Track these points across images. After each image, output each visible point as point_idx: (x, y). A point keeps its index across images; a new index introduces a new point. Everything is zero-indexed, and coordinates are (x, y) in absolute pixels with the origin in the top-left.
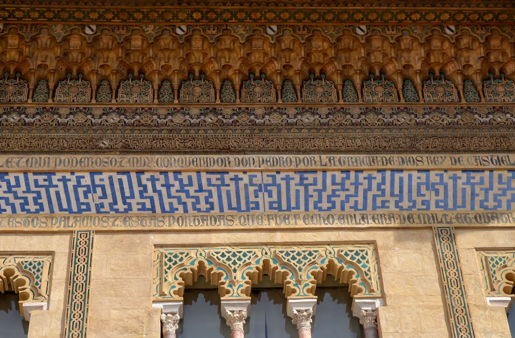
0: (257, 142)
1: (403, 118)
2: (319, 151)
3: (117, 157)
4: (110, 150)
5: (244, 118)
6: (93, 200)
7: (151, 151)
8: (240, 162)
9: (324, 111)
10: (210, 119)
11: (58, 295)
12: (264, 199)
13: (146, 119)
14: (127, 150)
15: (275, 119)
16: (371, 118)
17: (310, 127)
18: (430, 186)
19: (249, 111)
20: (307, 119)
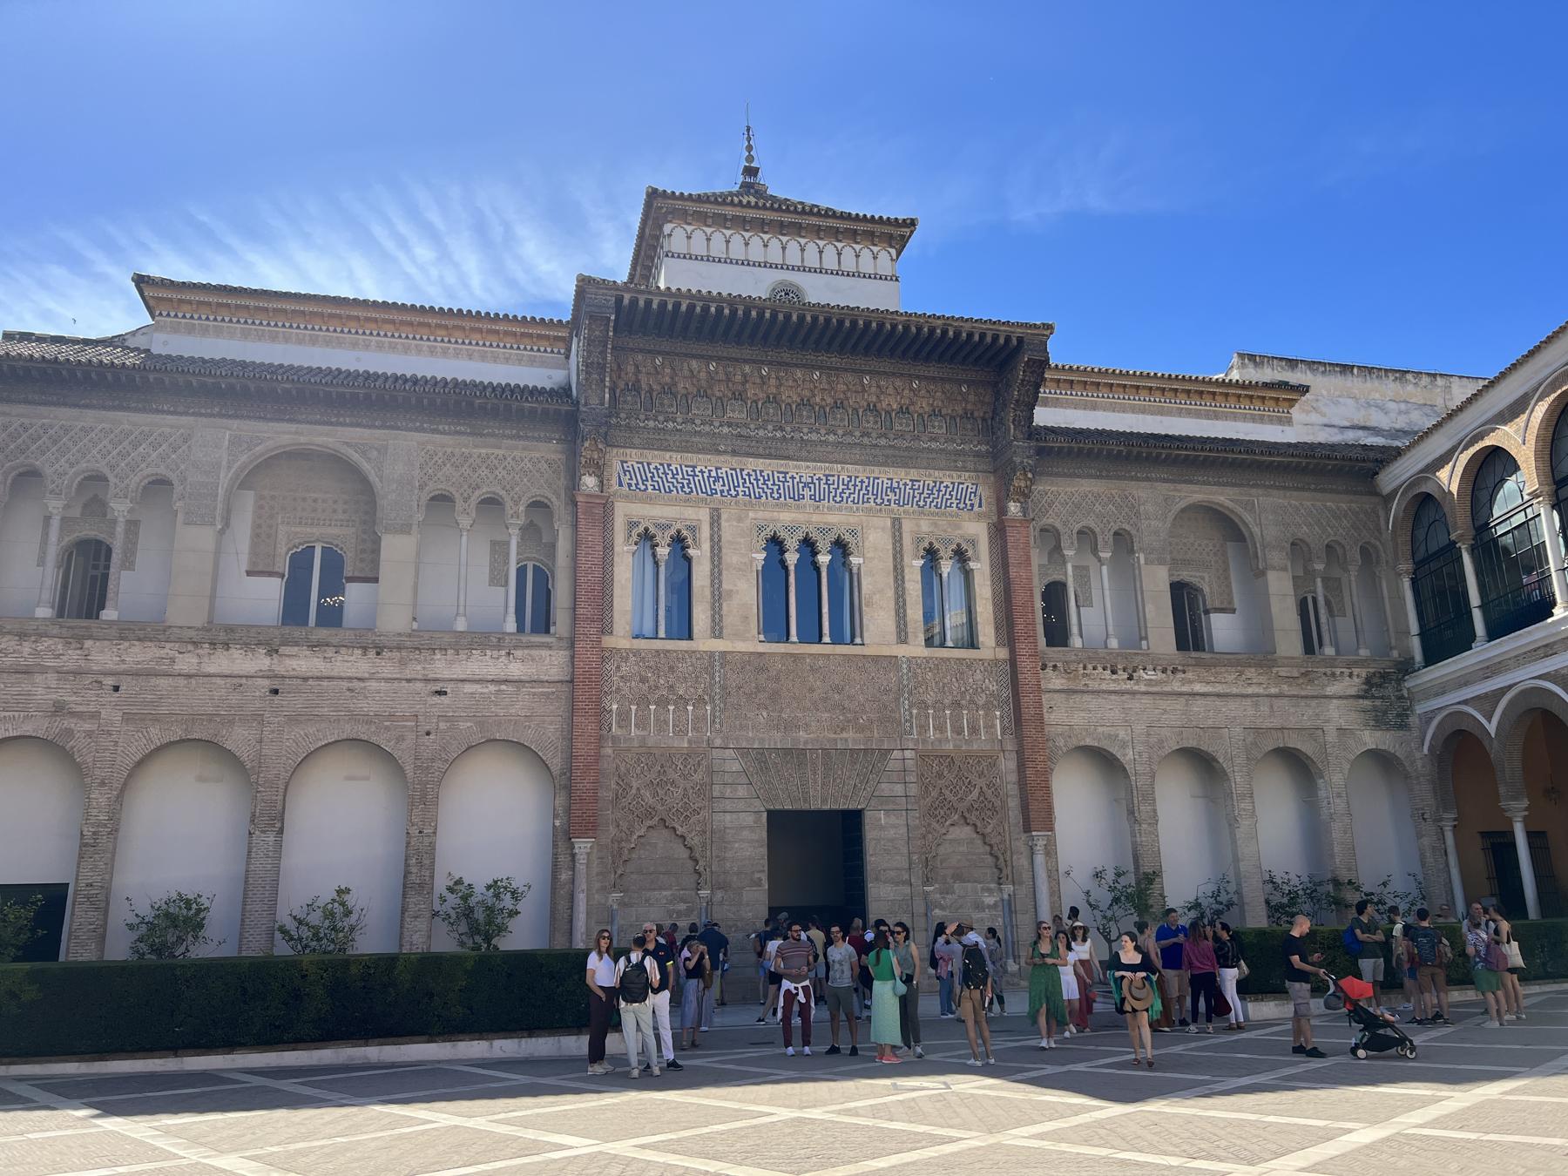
0: (804, 454)
1: (883, 442)
2: (837, 462)
3: (728, 458)
4: (725, 452)
5: (797, 435)
6: (718, 486)
9: (840, 432)
11: (706, 546)
12: (807, 492)
13: (744, 432)
14: (734, 453)
15: (814, 437)
16: (866, 440)
17: (833, 444)
18: (893, 490)
20: (831, 438)
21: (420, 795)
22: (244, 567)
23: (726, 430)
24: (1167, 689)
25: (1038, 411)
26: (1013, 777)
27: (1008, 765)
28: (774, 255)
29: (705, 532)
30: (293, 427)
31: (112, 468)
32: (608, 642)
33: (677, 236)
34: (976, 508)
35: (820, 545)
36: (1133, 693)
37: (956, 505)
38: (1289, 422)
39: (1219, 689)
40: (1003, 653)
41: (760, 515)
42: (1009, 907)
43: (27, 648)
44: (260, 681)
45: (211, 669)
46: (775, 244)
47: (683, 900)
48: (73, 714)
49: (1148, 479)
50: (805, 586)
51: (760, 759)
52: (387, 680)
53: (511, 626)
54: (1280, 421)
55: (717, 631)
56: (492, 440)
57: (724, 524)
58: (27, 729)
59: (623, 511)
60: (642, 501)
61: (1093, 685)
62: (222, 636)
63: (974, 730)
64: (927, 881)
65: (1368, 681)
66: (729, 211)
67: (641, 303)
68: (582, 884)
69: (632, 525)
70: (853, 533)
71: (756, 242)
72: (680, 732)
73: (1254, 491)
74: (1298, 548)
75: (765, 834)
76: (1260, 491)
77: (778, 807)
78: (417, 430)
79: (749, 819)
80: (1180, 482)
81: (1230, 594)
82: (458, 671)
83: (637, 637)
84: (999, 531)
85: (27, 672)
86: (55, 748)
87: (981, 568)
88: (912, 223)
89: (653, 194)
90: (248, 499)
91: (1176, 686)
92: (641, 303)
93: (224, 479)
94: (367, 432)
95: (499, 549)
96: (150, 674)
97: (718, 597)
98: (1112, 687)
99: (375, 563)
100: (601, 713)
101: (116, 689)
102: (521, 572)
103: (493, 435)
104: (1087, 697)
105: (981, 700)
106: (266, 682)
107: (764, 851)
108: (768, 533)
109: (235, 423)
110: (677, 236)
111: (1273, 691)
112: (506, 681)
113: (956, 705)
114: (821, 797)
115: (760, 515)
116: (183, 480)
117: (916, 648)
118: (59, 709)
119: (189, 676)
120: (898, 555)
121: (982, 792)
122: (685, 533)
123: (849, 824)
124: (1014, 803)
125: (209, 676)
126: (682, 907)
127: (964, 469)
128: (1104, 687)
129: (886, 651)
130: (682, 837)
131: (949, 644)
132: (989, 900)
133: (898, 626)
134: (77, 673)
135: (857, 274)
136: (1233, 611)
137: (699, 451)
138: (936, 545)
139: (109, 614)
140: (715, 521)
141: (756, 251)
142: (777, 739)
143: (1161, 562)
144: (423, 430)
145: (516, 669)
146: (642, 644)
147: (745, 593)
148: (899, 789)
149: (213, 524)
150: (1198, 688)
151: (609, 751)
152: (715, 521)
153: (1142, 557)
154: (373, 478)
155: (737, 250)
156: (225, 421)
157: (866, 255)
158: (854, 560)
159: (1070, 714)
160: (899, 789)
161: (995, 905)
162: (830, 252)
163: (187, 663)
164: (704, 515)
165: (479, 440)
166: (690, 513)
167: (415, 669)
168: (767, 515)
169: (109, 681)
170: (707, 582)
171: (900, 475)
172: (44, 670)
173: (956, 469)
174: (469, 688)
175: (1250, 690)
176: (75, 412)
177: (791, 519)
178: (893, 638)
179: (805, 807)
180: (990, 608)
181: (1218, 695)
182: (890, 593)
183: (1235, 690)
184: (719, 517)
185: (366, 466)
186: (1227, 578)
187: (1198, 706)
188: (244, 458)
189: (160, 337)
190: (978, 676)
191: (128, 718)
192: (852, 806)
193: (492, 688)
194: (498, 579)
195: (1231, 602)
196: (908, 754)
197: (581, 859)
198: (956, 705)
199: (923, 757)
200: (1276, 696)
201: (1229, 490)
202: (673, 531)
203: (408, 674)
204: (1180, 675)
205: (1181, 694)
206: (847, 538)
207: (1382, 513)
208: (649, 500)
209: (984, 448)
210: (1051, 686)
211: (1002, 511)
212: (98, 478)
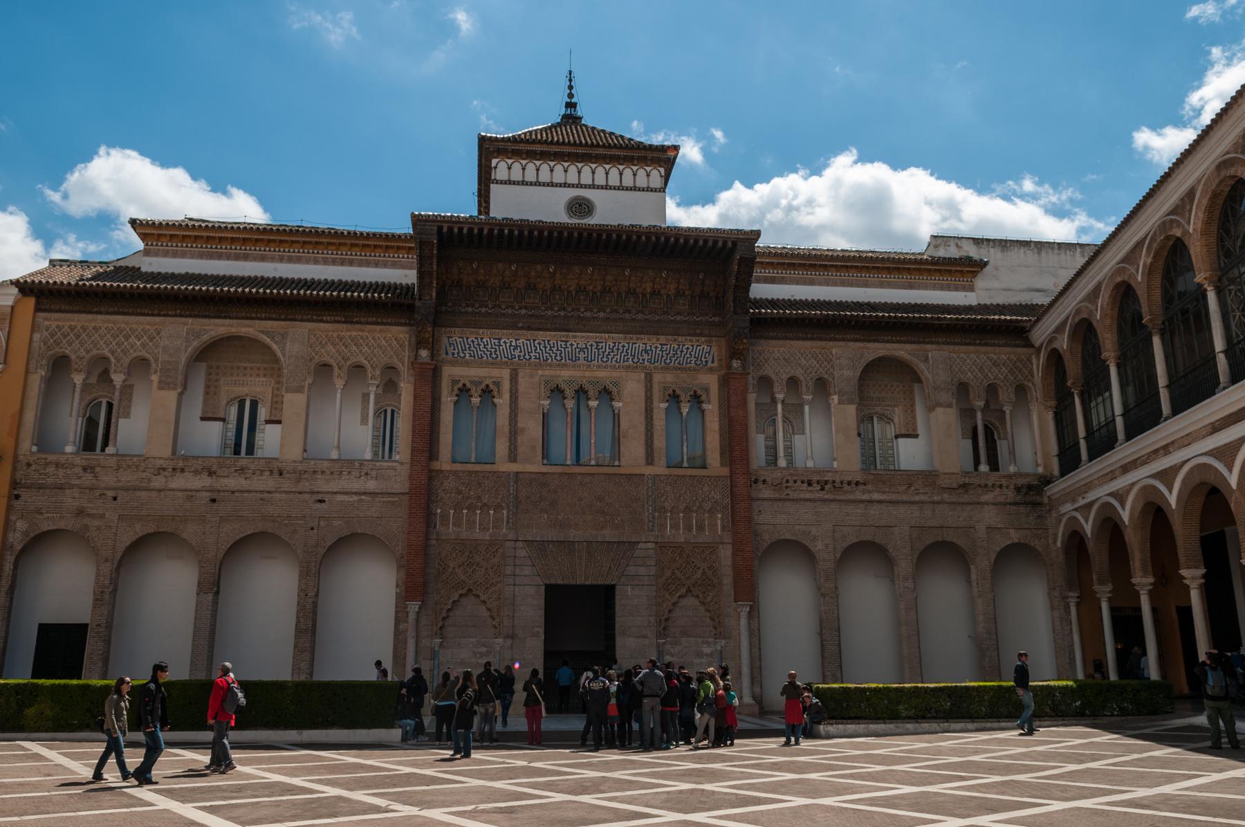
1: (640, 316)
5: (575, 314)
6: (517, 353)
7: (539, 329)
8: (574, 337)
10: (562, 313)
11: (507, 396)
12: (582, 356)
14: (529, 328)
15: (588, 314)
16: (627, 316)
18: (646, 351)
19: (578, 310)
20: (601, 315)
22: (199, 414)
23: (523, 312)
24: (852, 497)
26: (729, 562)
27: (726, 554)
28: (572, 177)
29: (506, 386)
30: (227, 321)
31: (113, 353)
32: (436, 465)
33: (501, 168)
34: (710, 364)
35: (591, 393)
36: (824, 501)
38: (972, 289)
39: (893, 497)
40: (725, 471)
41: (547, 373)
43: (61, 472)
44: (205, 494)
45: (173, 485)
47: (484, 645)
48: (89, 515)
49: (843, 340)
51: (539, 547)
52: (286, 492)
54: (964, 289)
55: (513, 458)
56: (359, 326)
57: (520, 380)
59: (449, 372)
60: (462, 365)
61: (793, 495)
62: (181, 464)
63: (701, 528)
65: (1018, 489)
66: (538, 148)
67: (456, 230)
69: (454, 382)
70: (616, 384)
71: (559, 169)
73: (929, 347)
74: (963, 389)
75: (543, 601)
76: (934, 347)
77: (553, 582)
78: (308, 321)
80: (869, 341)
81: (915, 424)
82: (334, 486)
83: (454, 462)
84: (725, 382)
85: (61, 488)
87: (712, 408)
89: (482, 140)
90: (202, 368)
91: (859, 496)
92: (456, 230)
93: (183, 359)
94: (275, 323)
96: (136, 489)
97: (514, 432)
98: (808, 496)
101: (115, 499)
103: (360, 323)
104: (787, 504)
105: (707, 506)
106: (208, 494)
107: (542, 612)
109: (190, 320)
110: (501, 168)
111: (936, 498)
112: (364, 493)
113: (688, 510)
114: (583, 575)
115: (547, 373)
116: (156, 360)
118: (80, 512)
119: (159, 491)
120: (649, 399)
121: (704, 573)
122: (491, 386)
123: (608, 593)
124: (728, 581)
125: (172, 490)
126: (484, 649)
127: (701, 335)
128: (802, 496)
130: (484, 602)
131: (685, 464)
132: (707, 650)
133: (647, 452)
134: (92, 489)
135: (635, 188)
136: (916, 436)
137: (503, 328)
138: (678, 392)
139: (110, 450)
140: (514, 378)
141: (559, 176)
142: (552, 535)
143: (850, 402)
144: (313, 321)
145: (371, 485)
146: (458, 467)
149: (175, 389)
150: (876, 496)
151: (434, 542)
152: (514, 378)
153: (836, 398)
154: (279, 354)
155: (545, 176)
156: (183, 319)
157: (641, 173)
160: (642, 571)
161: (711, 654)
163: (158, 482)
164: (505, 374)
165: (349, 326)
166: (496, 372)
167: (304, 485)
168: (552, 373)
169: (111, 494)
170: (507, 422)
172: (72, 487)
173: (695, 335)
174: (340, 498)
175: (917, 498)
176: (90, 316)
178: (643, 461)
179: (573, 582)
180: (717, 437)
181: (891, 502)
182: (642, 428)
183: (904, 498)
184: (517, 375)
185: (274, 347)
186: (913, 411)
187: (874, 510)
188: (195, 343)
189: (148, 259)
190: (706, 489)
191: (121, 518)
192: (608, 582)
193: (355, 498)
195: (915, 429)
196: (650, 545)
198: (688, 510)
199: (662, 546)
200: (938, 503)
201: (908, 347)
202: (483, 386)
203: (300, 487)
204: (861, 487)
205: (861, 501)
207: (1034, 361)
208: (467, 364)
209: (717, 319)
210: (761, 496)
211: (729, 367)
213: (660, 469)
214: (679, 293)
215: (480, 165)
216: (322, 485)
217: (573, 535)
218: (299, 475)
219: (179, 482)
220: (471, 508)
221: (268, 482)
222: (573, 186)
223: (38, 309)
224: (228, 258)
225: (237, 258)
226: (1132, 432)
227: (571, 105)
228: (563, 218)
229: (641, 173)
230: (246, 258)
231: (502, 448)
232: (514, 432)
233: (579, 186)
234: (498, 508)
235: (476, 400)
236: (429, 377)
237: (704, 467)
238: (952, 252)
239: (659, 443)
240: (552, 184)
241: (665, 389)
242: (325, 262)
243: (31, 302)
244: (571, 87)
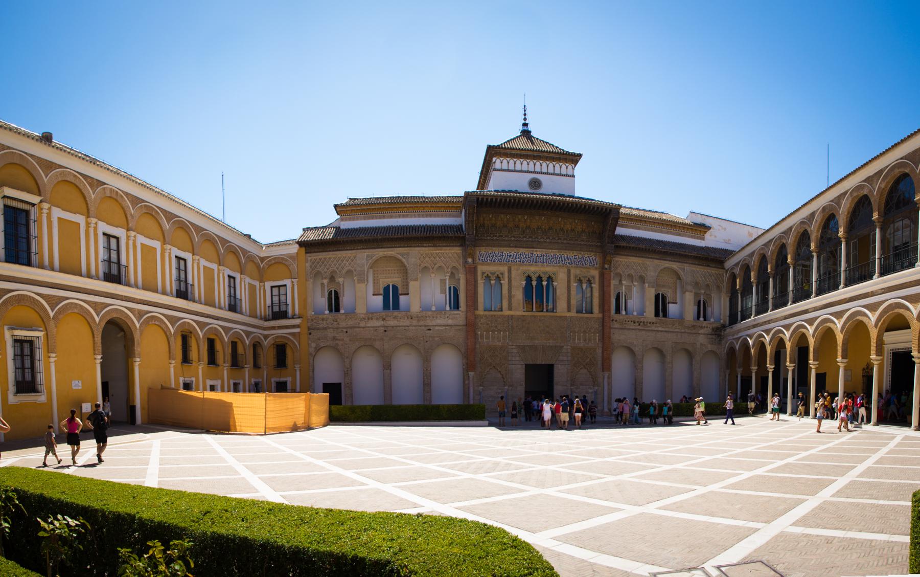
21: (426, 360)
25: (618, 228)
27: (599, 351)
28: (531, 169)
33: (498, 162)
37: (587, 263)
40: (601, 315)
42: (596, 393)
46: (531, 163)
50: (537, 291)
51: (522, 348)
53: (448, 308)
55: (510, 308)
58: (328, 344)
63: (590, 340)
64: (572, 385)
68: (471, 384)
70: (554, 274)
72: (499, 341)
79: (519, 366)
84: (602, 275)
85: (325, 329)
86: (335, 349)
87: (596, 286)
88: (580, 155)
95: (443, 282)
96: (355, 327)
97: (510, 297)
99: (407, 289)
100: (476, 334)
102: (450, 288)
108: (526, 275)
110: (498, 162)
113: (585, 332)
114: (541, 360)
117: (573, 314)
118: (334, 338)
120: (569, 281)
129: (563, 314)
134: (337, 328)
135: (560, 175)
139: (342, 311)
141: (525, 167)
145: (450, 322)
146: (487, 313)
147: (519, 295)
148: (565, 358)
155: (518, 167)
157: (564, 166)
158: (555, 284)
159: (618, 336)
160: (565, 358)
162: (551, 166)
171: (571, 254)
177: (534, 269)
182: (566, 295)
191: (350, 340)
194: (443, 291)
197: (471, 378)
198: (585, 332)
206: (552, 276)
212: (334, 272)
213: (573, 314)
214: (583, 231)
215: (485, 160)
216: (429, 322)
217: (536, 342)
218: (419, 318)
219: (371, 324)
220: (493, 331)
221: (407, 323)
222: (531, 172)
223: (306, 253)
224: (377, 218)
225: (380, 218)
226: (758, 313)
227: (525, 125)
228: (528, 189)
229: (564, 166)
230: (384, 217)
231: (505, 304)
232: (510, 297)
233: (534, 172)
234: (505, 331)
235: (493, 282)
236: (471, 272)
237: (592, 313)
238: (699, 220)
239: (573, 302)
240: (521, 171)
241: (576, 276)
242: (419, 216)
243: (303, 249)
244: (525, 115)
